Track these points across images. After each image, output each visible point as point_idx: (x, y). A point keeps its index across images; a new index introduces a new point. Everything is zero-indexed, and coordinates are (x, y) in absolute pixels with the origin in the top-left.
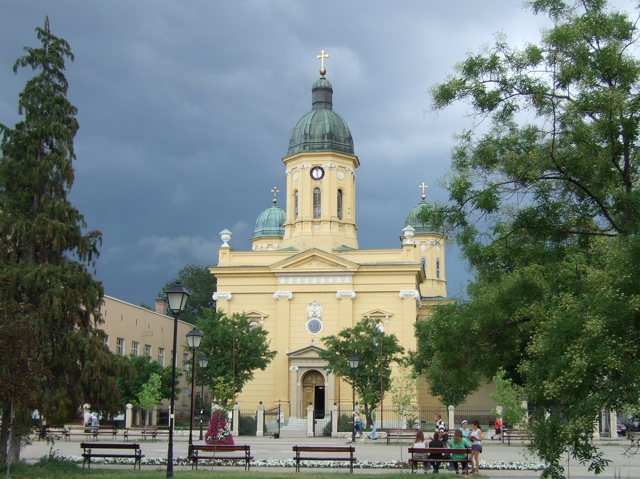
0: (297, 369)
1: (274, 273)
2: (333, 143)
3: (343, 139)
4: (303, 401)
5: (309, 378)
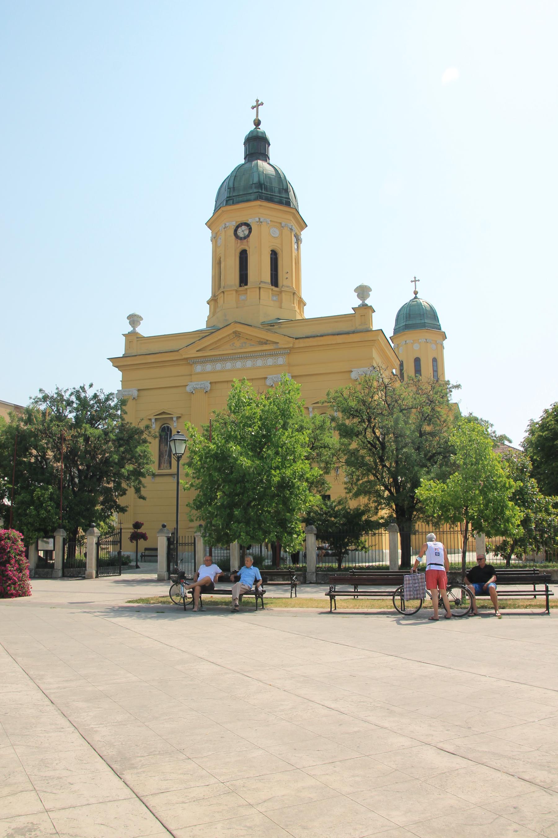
2: (262, 193)
3: (277, 190)
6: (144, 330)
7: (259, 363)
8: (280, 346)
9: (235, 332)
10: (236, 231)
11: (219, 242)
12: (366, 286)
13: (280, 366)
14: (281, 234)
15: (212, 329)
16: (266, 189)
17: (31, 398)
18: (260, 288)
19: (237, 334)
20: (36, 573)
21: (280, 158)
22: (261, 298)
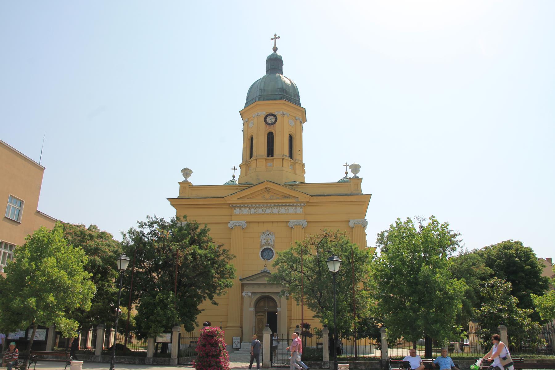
0: (250, 294)
1: (229, 204)
3: (293, 94)
4: (255, 326)
5: (262, 304)
6: (194, 180)
7: (283, 210)
8: (300, 200)
9: (266, 188)
10: (265, 119)
11: (251, 125)
12: (358, 165)
13: (298, 214)
14: (295, 124)
15: (245, 185)
16: (286, 93)
17: (138, 222)
18: (283, 159)
19: (267, 190)
20: (154, 361)
21: (289, 74)
22: (284, 166)
